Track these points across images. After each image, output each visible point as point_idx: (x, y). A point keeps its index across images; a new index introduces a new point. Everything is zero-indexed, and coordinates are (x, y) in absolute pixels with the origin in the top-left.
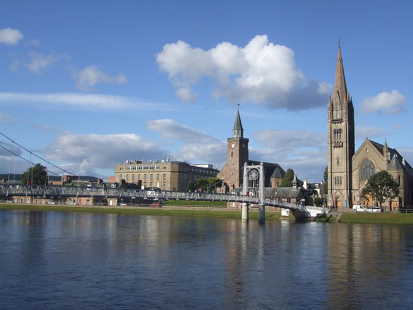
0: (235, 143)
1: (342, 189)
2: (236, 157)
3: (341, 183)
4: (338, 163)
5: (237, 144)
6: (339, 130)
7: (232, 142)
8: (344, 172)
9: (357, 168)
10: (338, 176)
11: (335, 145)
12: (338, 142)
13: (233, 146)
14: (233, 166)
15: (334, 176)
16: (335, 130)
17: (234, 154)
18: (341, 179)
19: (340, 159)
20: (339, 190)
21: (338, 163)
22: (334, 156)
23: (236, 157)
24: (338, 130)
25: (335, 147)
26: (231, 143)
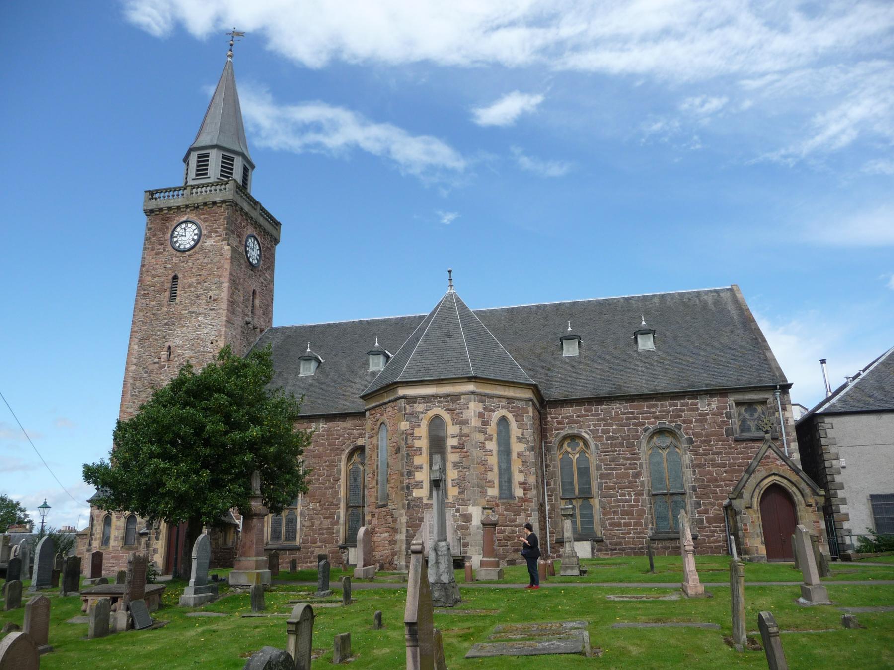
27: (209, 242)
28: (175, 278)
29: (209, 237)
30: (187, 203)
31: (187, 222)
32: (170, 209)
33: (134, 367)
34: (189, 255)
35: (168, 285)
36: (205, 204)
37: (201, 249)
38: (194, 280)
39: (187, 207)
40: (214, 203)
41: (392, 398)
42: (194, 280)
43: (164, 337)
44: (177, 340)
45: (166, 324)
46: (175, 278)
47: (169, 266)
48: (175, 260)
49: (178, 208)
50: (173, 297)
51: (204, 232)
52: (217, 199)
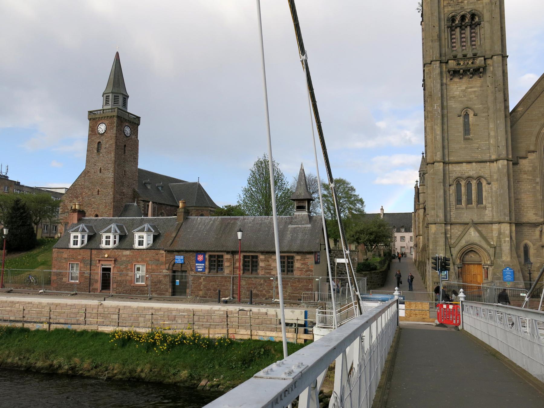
0: (107, 122)
1: (487, 219)
2: (109, 153)
3: (480, 200)
4: (467, 129)
5: (112, 123)
6: (468, 16)
7: (99, 121)
8: (492, 161)
9: (532, 148)
10: (467, 175)
11: (457, 67)
12: (465, 56)
13: (102, 128)
14: (100, 175)
15: (454, 175)
16: (453, 19)
17: (103, 146)
18: (479, 185)
19: (475, 115)
20: (475, 224)
21: (467, 129)
22: (454, 106)
23: (109, 153)
24: (463, 17)
25: (455, 73)
26: (96, 123)
27: (133, 137)
28: (125, 146)
29: (133, 135)
30: (129, 119)
31: (128, 126)
32: (124, 118)
33: (116, 175)
34: (128, 139)
35: (123, 148)
36: (133, 122)
37: (131, 138)
38: (130, 149)
39: (128, 120)
40: (135, 123)
41: (207, 209)
42: (130, 149)
43: (124, 166)
44: (127, 168)
45: (124, 162)
46: (125, 146)
47: (123, 140)
48: (125, 139)
49: (126, 120)
50: (125, 153)
51: (132, 133)
52: (136, 122)
